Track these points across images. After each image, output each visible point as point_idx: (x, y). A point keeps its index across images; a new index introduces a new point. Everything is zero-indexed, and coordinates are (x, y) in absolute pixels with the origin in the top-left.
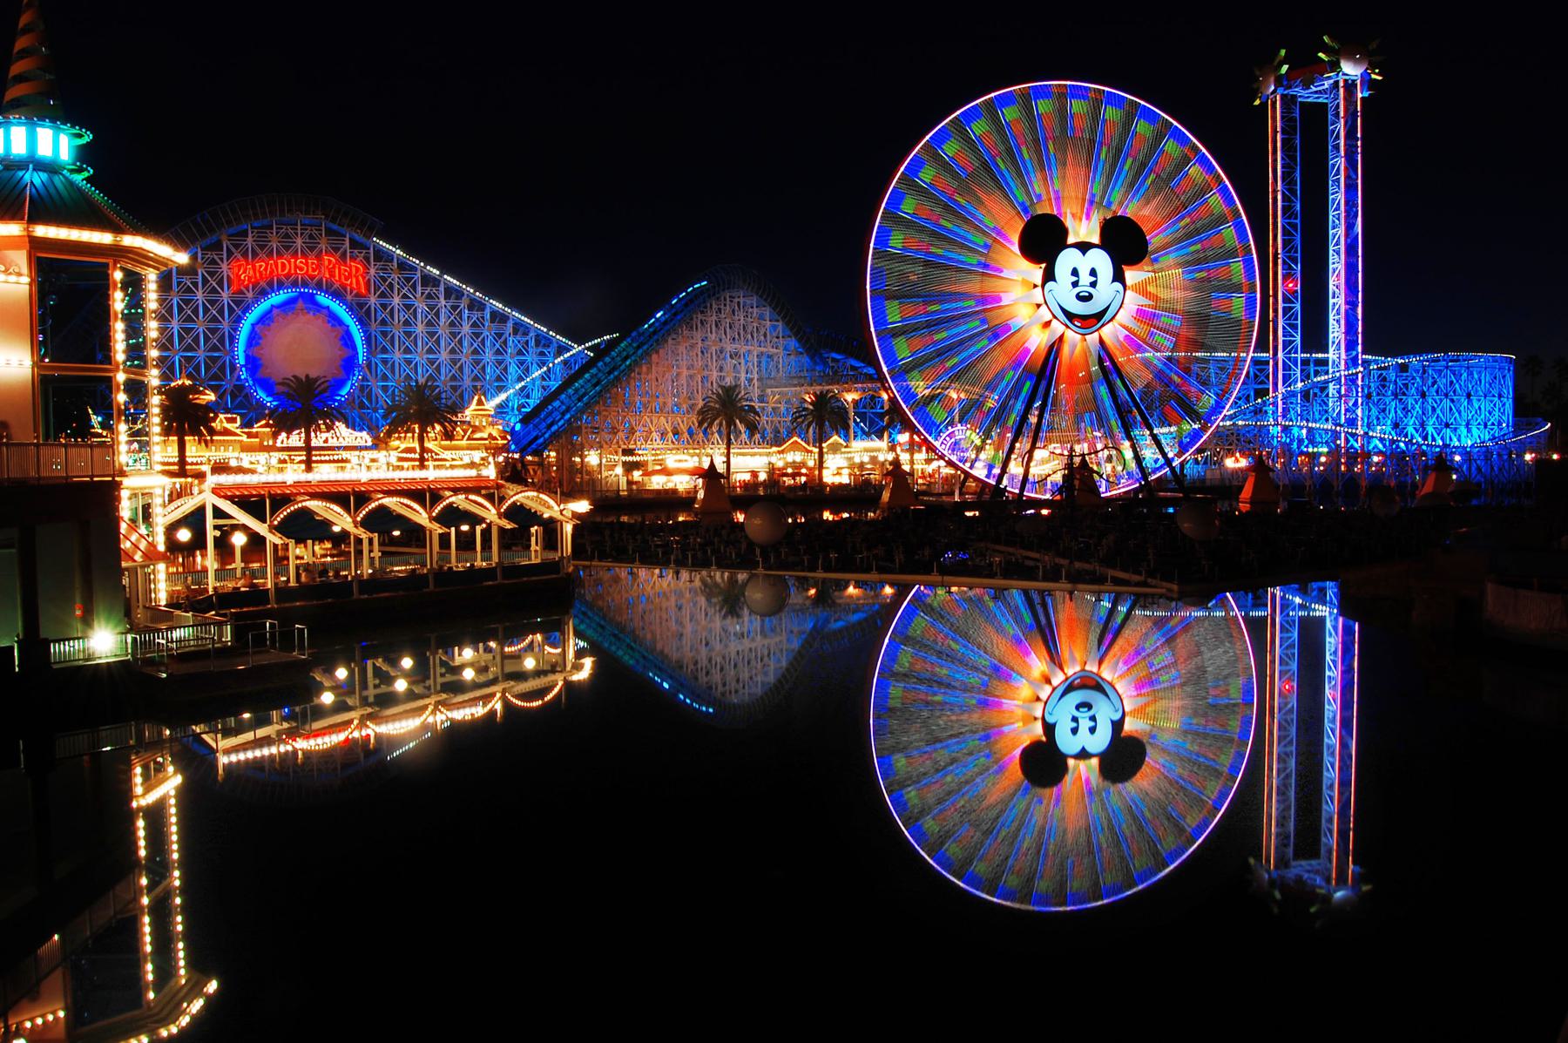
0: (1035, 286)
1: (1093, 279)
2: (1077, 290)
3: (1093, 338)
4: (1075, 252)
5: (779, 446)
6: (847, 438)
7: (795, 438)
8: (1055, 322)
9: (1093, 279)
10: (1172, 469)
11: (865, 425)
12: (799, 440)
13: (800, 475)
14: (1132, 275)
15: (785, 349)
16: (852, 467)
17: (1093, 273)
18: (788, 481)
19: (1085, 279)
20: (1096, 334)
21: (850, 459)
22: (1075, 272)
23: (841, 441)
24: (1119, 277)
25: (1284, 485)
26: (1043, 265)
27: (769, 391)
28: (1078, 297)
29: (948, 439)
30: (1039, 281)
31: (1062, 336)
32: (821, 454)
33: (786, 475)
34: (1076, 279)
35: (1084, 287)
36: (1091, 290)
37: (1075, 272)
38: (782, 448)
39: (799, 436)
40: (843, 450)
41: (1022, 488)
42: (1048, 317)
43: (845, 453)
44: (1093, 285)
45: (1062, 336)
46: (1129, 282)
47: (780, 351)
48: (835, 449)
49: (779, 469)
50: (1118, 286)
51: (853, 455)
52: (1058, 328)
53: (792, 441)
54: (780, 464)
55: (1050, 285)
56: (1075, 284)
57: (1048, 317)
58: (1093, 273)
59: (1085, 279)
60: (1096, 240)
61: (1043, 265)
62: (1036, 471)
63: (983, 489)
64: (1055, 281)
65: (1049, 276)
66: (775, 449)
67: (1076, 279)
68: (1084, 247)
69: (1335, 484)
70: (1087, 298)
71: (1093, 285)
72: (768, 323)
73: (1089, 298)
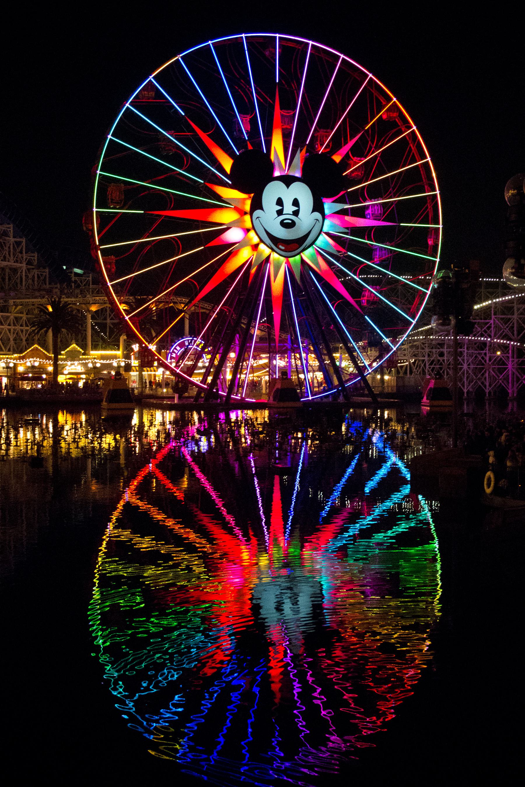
0: (246, 213)
1: (297, 208)
3: (295, 260)
4: (280, 185)
5: (21, 352)
6: (84, 346)
7: (36, 346)
8: (262, 247)
9: (296, 208)
10: (364, 378)
11: (105, 334)
12: (39, 348)
13: (41, 379)
14: (329, 207)
15: (29, 263)
16: (88, 372)
17: (296, 203)
18: (27, 386)
19: (289, 208)
20: (298, 258)
21: (85, 365)
22: (280, 202)
23: (79, 349)
24: (318, 207)
25: (467, 392)
26: (252, 195)
27: (11, 302)
29: (178, 348)
30: (248, 208)
31: (269, 257)
32: (56, 360)
33: (28, 379)
34: (279, 208)
36: (293, 218)
38: (24, 354)
39: (39, 344)
40: (81, 357)
41: (230, 392)
42: (255, 240)
43: (82, 359)
44: (296, 213)
45: (269, 257)
46: (327, 212)
47: (24, 266)
48: (73, 356)
49: (20, 374)
50: (317, 215)
51: (87, 361)
52: (264, 250)
53: (32, 347)
54: (21, 369)
56: (280, 213)
57: (255, 240)
58: (296, 203)
59: (289, 208)
60: (298, 174)
61: (252, 195)
62: (246, 377)
63: (199, 393)
64: (262, 209)
65: (257, 205)
66: (16, 355)
67: (279, 208)
68: (288, 180)
69: (510, 391)
70: (288, 225)
71: (296, 213)
72: (12, 240)
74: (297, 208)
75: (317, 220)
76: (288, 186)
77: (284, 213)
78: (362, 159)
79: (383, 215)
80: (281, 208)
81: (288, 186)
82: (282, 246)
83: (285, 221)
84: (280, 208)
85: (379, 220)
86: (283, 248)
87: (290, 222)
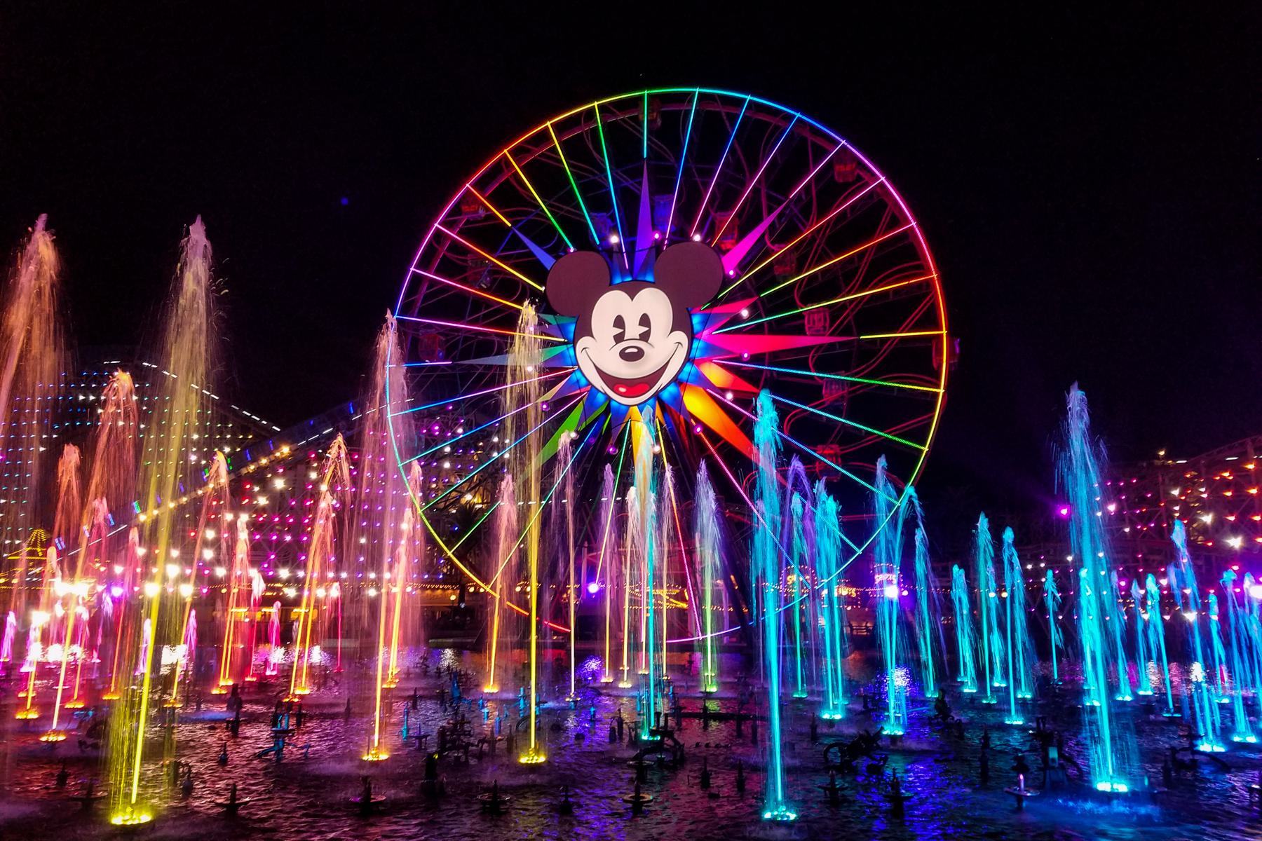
2: (622, 345)
17: (645, 321)
19: (634, 329)
22: (619, 322)
24: (681, 322)
28: (625, 356)
35: (631, 342)
36: (642, 344)
37: (619, 322)
44: (645, 337)
50: (681, 337)
55: (583, 342)
56: (619, 338)
58: (645, 321)
59: (634, 329)
65: (584, 329)
67: (621, 331)
73: (638, 355)
74: (647, 329)
75: (679, 343)
76: (632, 297)
77: (625, 338)
78: (782, 245)
79: (831, 327)
80: (621, 331)
81: (632, 297)
82: (623, 387)
83: (627, 351)
84: (621, 331)
85: (824, 335)
86: (622, 390)
87: (636, 350)
